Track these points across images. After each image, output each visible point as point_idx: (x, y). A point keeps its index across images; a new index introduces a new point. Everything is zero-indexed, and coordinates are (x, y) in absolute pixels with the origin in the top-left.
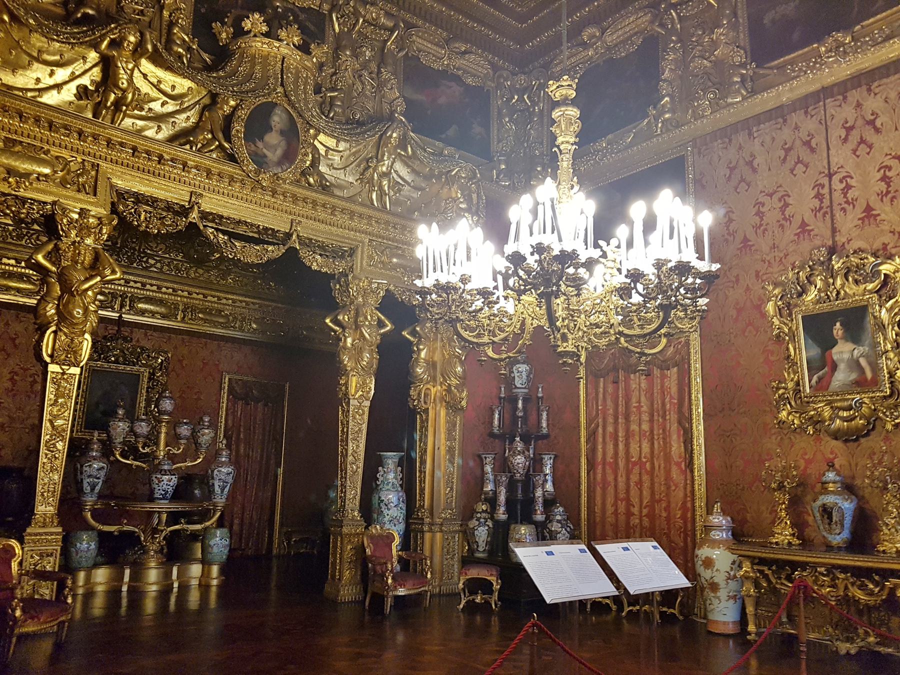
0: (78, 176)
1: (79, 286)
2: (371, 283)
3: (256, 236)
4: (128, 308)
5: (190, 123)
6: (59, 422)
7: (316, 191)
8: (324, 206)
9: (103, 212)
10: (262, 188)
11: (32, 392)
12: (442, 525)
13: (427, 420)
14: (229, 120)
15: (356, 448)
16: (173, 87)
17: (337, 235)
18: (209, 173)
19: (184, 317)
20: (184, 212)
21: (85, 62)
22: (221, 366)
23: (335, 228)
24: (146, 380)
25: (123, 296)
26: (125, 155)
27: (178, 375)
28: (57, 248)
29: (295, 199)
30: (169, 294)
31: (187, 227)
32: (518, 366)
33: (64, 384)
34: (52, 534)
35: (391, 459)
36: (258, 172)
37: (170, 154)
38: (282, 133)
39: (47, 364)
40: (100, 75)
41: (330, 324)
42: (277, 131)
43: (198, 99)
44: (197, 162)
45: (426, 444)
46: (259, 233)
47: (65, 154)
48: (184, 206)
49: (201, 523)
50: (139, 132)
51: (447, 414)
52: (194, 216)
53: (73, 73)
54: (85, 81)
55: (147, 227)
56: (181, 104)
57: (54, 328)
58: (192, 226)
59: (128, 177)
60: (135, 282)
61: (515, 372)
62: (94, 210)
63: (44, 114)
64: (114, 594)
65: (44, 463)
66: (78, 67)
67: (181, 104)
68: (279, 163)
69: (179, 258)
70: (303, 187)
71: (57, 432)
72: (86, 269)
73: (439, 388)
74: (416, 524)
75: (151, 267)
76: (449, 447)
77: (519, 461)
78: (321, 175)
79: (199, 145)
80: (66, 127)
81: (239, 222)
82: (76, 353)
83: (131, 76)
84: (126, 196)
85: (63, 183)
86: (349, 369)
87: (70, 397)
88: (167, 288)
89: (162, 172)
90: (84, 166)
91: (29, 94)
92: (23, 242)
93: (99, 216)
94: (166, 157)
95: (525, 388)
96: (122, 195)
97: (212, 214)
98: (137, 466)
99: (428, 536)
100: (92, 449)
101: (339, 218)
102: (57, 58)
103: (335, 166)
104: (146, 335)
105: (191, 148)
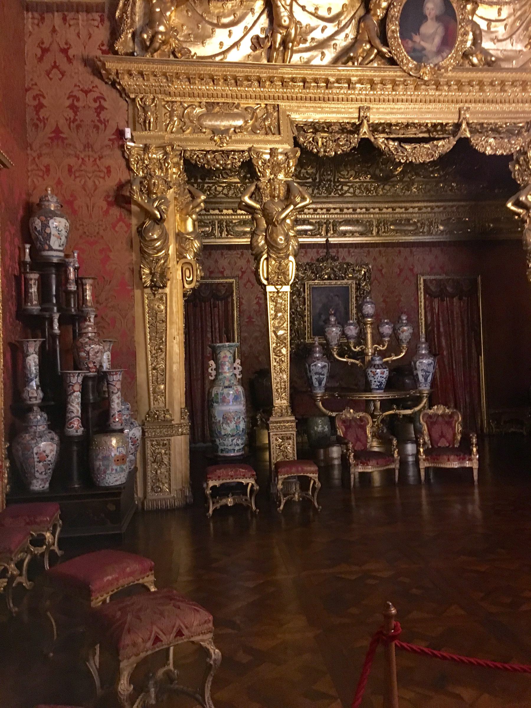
0: (264, 120)
1: (278, 217)
3: (426, 135)
4: (332, 232)
5: (349, 40)
6: (280, 333)
7: (481, 71)
8: (492, 84)
10: (426, 83)
14: (383, 23)
16: (329, 9)
17: (510, 112)
18: (372, 83)
19: (378, 232)
20: (356, 128)
21: (253, 13)
22: (416, 270)
23: (507, 105)
24: (354, 290)
25: (327, 223)
26: (297, 90)
28: (258, 188)
29: (460, 85)
30: (363, 214)
31: (359, 143)
33: (280, 301)
34: (288, 422)
36: (418, 68)
37: (334, 75)
38: (438, 19)
39: (265, 286)
40: (267, 21)
41: (513, 208)
42: (432, 19)
43: (353, 13)
44: (360, 76)
46: (428, 131)
47: (252, 103)
48: (354, 124)
49: (410, 408)
50: (307, 65)
52: (365, 129)
53: (246, 27)
54: (256, 31)
55: (325, 151)
56: (339, 24)
57: (265, 256)
58: (365, 143)
59: (304, 109)
60: (335, 209)
62: (281, 148)
63: (229, 72)
65: (275, 366)
66: (249, 20)
67: (339, 24)
68: (439, 52)
69: (368, 180)
70: (468, 70)
71: (280, 340)
72: (281, 200)
78: (486, 53)
79: (360, 59)
80: (247, 79)
81: (407, 125)
82: (285, 274)
83: (291, 12)
84: (305, 128)
85: (254, 131)
87: (286, 311)
88: (361, 209)
89: (330, 96)
90: (267, 110)
91: (218, 59)
93: (285, 152)
94: (332, 79)
96: (301, 128)
97: (381, 124)
98: (352, 363)
100: (316, 353)
101: (510, 93)
102: (232, 18)
103: (500, 37)
105: (353, 64)
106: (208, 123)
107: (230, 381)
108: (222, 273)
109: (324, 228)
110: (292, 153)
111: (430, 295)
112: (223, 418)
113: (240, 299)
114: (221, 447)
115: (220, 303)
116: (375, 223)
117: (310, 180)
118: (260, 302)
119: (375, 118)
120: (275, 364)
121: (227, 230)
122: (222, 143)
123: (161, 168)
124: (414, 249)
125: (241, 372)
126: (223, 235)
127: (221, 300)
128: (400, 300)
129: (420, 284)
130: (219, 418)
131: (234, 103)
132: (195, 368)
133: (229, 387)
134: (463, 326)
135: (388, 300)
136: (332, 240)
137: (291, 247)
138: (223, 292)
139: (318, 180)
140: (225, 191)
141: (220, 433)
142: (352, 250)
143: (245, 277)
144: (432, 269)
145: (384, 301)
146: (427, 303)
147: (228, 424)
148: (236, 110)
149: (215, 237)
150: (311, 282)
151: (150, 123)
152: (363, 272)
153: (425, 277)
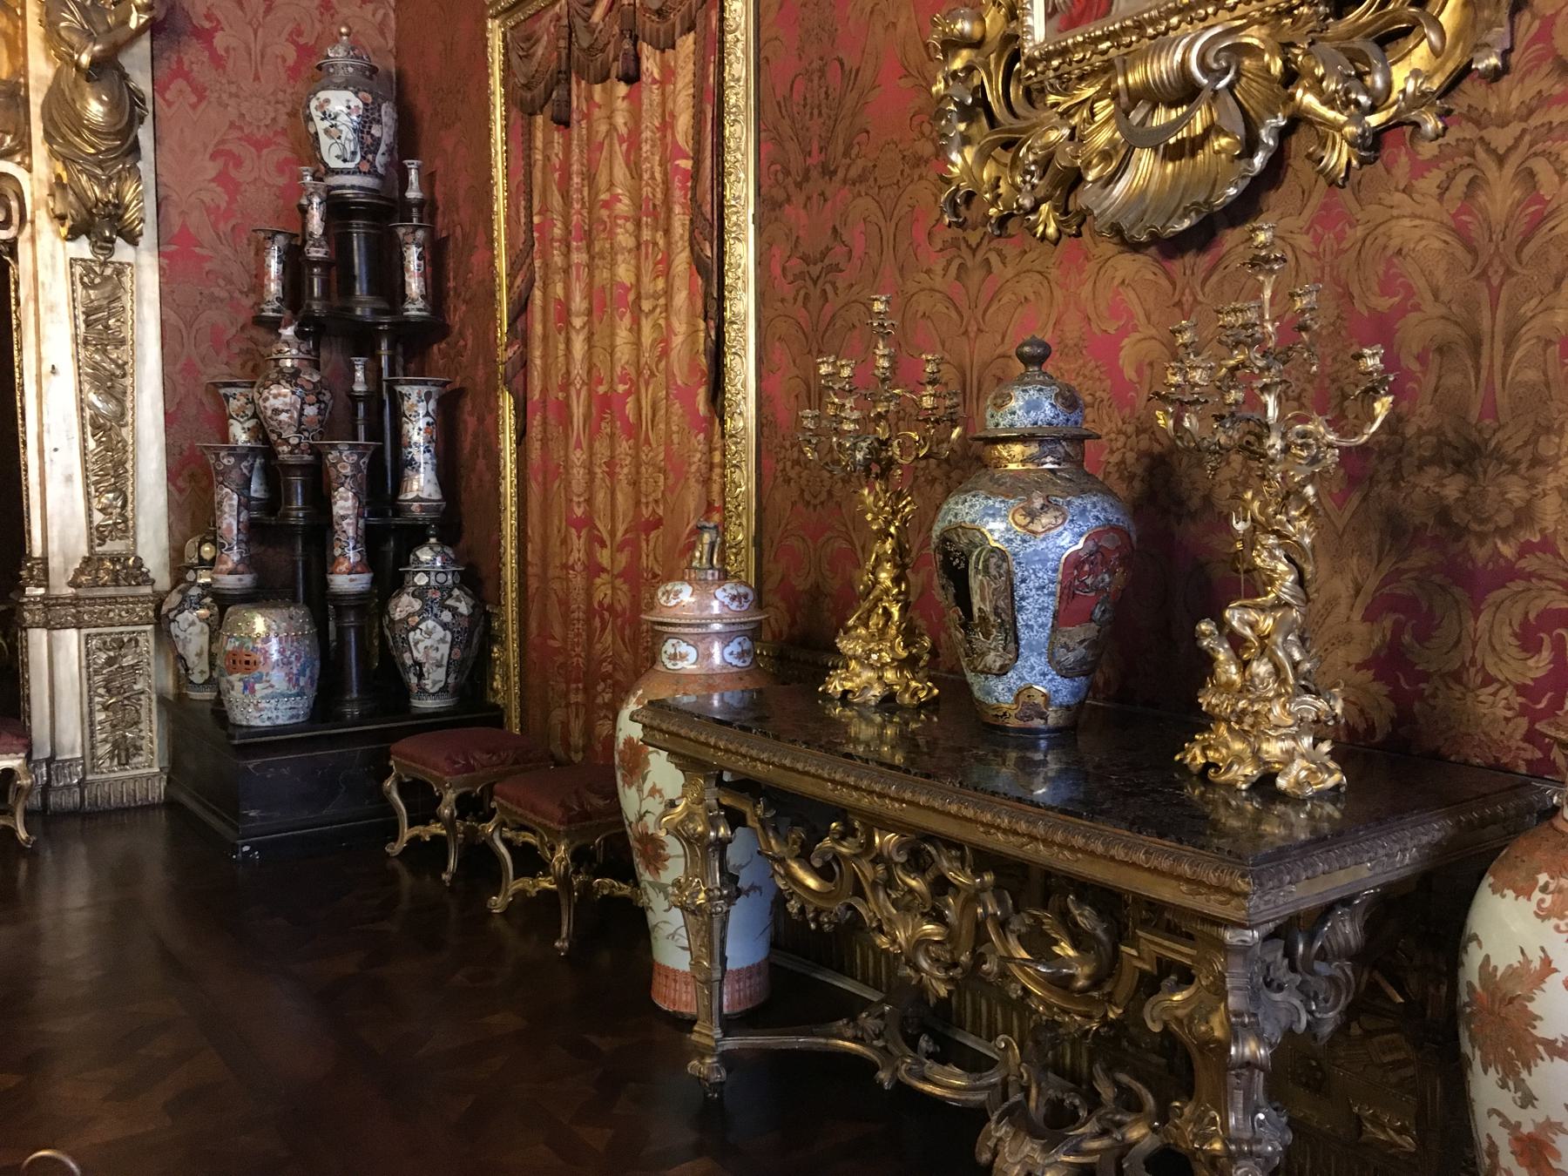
32: (322, 95)
61: (316, 115)
77: (278, 403)
95: (357, 171)
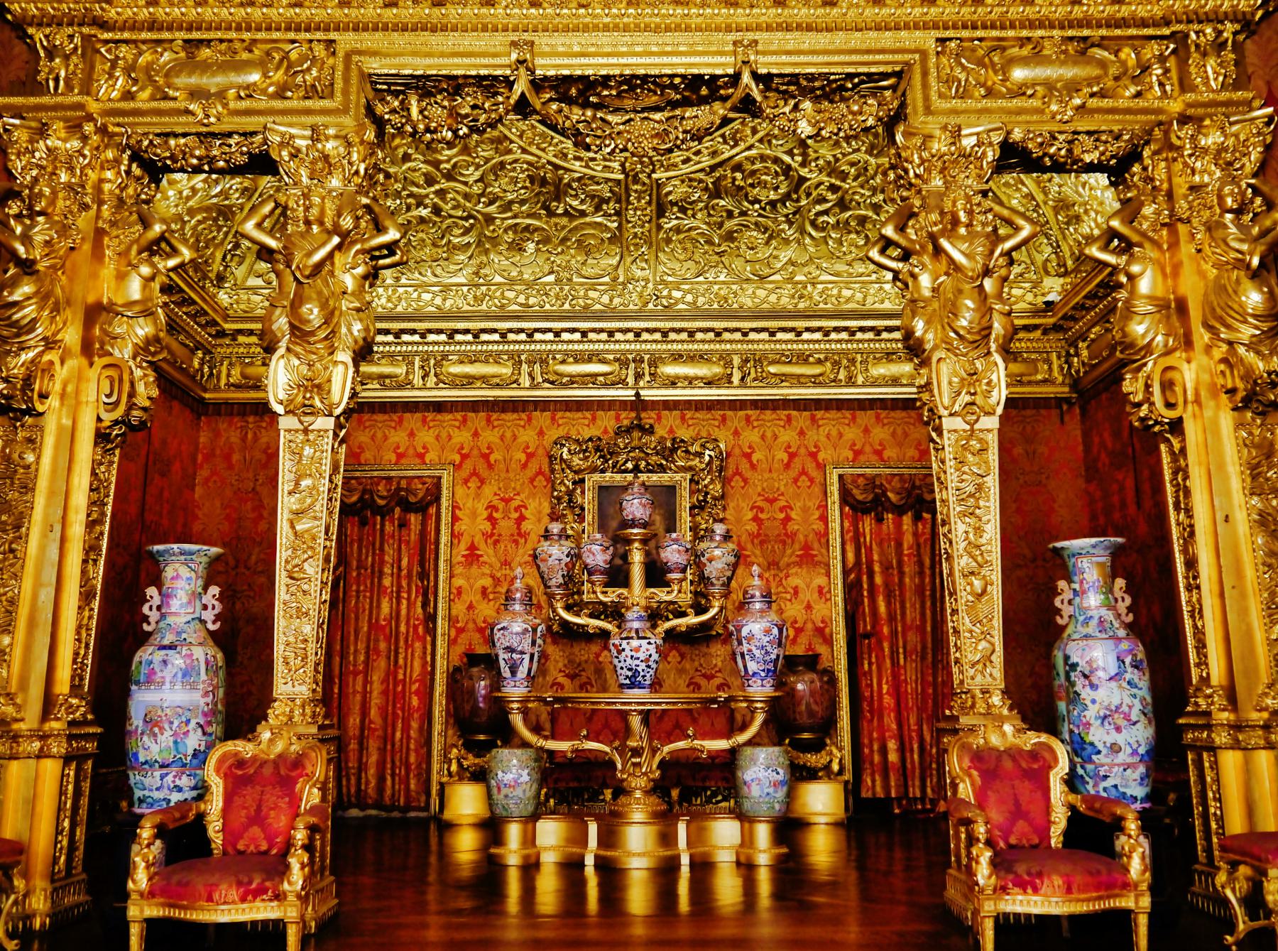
2: (957, 134)
4: (647, 378)
9: (348, 121)
11: (520, 534)
12: (1266, 727)
13: (1183, 451)
15: (974, 535)
19: (743, 379)
22: (821, 456)
24: (686, 494)
27: (745, 481)
35: (1088, 556)
45: (1189, 513)
49: (728, 736)
51: (1239, 425)
64: (571, 868)
69: (722, 278)
73: (1204, 360)
74: (1194, 727)
75: (676, 304)
76: (1261, 513)
85: (280, 95)
86: (928, 347)
92: (484, 307)
93: (343, 133)
99: (1230, 761)
104: (683, 418)
106: (183, 80)
107: (179, 634)
108: (421, 456)
109: (631, 372)
110: (357, 133)
111: (852, 507)
112: (145, 721)
113: (455, 507)
114: (138, 794)
115: (414, 519)
116: (736, 361)
117: (607, 279)
118: (495, 515)
119: (547, 67)
120: (287, 597)
121: (436, 375)
122: (208, 116)
123: (71, 169)
124: (819, 414)
125: (218, 618)
126: (428, 385)
127: (416, 512)
128: (788, 519)
129: (832, 484)
130: (137, 721)
131: (243, 41)
132: (352, 649)
133: (172, 647)
134: (921, 573)
135: (762, 516)
136: (647, 394)
137: (344, 330)
138: (421, 495)
139: (621, 280)
140: (438, 301)
141: (136, 755)
142: (689, 414)
143: (468, 466)
144: (857, 453)
145: (755, 519)
146: (846, 524)
147: (155, 735)
148: (245, 56)
149: (413, 388)
150: (597, 477)
151: (57, 80)
152: (707, 458)
153: (841, 471)
